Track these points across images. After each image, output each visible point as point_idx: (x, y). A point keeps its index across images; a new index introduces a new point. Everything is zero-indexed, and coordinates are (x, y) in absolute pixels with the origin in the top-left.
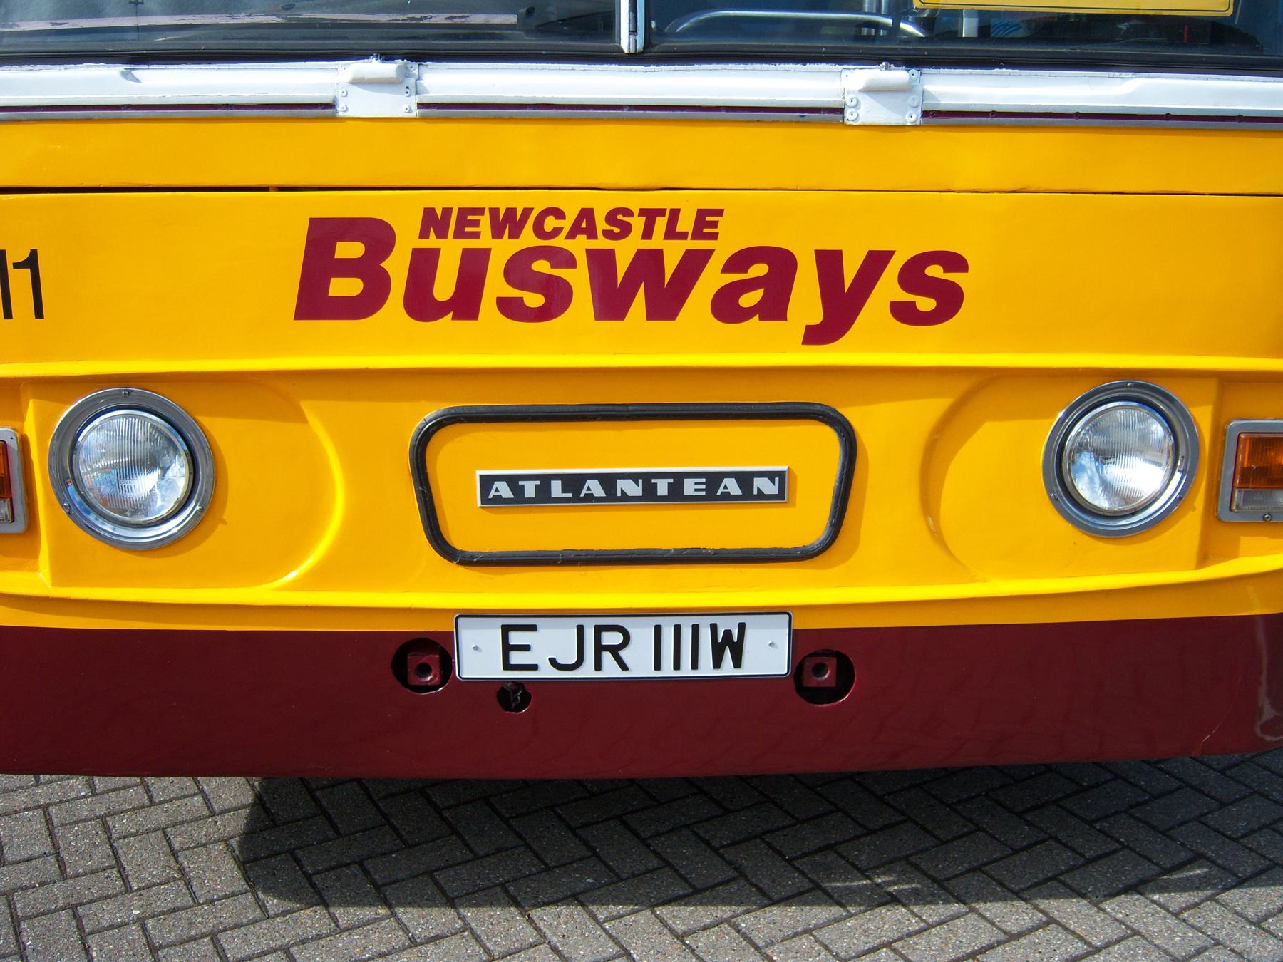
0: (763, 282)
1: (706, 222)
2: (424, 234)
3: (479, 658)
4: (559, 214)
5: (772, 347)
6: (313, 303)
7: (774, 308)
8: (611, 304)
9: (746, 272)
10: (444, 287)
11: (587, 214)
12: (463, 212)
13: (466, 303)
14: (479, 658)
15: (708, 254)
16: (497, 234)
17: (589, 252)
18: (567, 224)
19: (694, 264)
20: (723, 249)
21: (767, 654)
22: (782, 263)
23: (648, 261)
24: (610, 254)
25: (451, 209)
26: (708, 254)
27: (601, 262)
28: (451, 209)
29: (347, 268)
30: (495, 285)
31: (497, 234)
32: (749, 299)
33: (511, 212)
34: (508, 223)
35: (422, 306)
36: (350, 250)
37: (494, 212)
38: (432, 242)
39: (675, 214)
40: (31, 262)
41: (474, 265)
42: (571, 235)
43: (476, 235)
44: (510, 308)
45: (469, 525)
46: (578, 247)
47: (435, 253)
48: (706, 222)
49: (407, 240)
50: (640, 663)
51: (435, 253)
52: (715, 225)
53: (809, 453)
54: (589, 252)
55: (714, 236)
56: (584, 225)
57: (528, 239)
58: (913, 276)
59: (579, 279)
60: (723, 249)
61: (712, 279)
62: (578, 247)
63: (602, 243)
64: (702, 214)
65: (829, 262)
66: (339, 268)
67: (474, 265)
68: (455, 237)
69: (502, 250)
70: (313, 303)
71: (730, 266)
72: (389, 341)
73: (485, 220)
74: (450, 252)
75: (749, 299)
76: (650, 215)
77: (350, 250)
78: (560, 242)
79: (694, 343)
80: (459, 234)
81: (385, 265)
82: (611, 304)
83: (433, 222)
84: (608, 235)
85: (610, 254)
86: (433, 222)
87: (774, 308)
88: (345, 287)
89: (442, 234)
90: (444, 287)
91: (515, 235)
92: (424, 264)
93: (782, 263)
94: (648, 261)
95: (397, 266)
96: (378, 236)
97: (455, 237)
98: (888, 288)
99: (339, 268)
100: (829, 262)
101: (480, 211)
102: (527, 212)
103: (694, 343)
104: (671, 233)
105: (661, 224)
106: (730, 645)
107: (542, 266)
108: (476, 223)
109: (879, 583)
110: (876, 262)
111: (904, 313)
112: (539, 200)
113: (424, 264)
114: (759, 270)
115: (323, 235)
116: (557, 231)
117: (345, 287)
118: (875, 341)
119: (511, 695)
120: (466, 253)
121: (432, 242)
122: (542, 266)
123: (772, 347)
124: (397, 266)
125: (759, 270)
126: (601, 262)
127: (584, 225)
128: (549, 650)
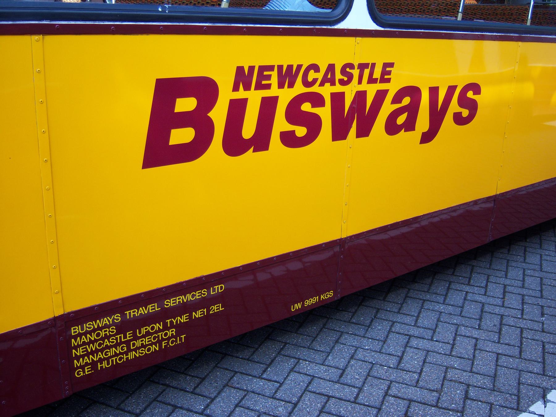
2: (236, 88)
4: (316, 68)
9: (400, 102)
11: (331, 68)
12: (262, 69)
13: (261, 142)
15: (385, 92)
16: (281, 85)
17: (332, 94)
18: (320, 76)
24: (342, 94)
25: (254, 67)
26: (385, 92)
28: (254, 67)
29: (184, 120)
30: (281, 124)
31: (281, 85)
32: (401, 120)
33: (290, 67)
35: (235, 145)
36: (186, 104)
37: (280, 67)
38: (241, 94)
39: (374, 65)
42: (322, 84)
43: (268, 87)
44: (289, 140)
46: (326, 91)
47: (245, 101)
51: (245, 101)
52: (389, 73)
54: (332, 94)
55: (388, 81)
56: (329, 76)
57: (299, 89)
59: (325, 113)
60: (393, 88)
62: (326, 91)
63: (338, 88)
64: (386, 65)
68: (256, 89)
70: (158, 153)
71: (394, 101)
73: (274, 74)
75: (401, 120)
76: (362, 67)
77: (186, 104)
78: (315, 89)
80: (259, 86)
81: (209, 115)
83: (242, 78)
84: (342, 82)
85: (342, 94)
86: (242, 78)
88: (182, 136)
89: (247, 88)
91: (291, 85)
95: (219, 115)
96: (205, 90)
97: (256, 89)
98: (454, 107)
101: (271, 68)
102: (299, 67)
104: (371, 80)
105: (367, 72)
107: (306, 107)
108: (269, 77)
114: (406, 101)
116: (315, 81)
117: (182, 136)
120: (265, 101)
121: (241, 94)
122: (306, 107)
124: (219, 115)
125: (406, 101)
127: (329, 76)
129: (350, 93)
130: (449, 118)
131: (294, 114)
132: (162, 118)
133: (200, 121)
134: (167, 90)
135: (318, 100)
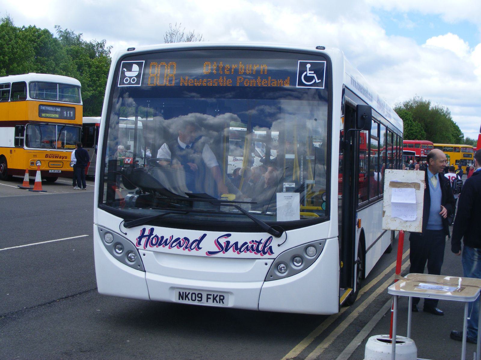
0: (60, 157)
1: (59, 155)
3: (50, 172)
5: (61, 159)
6: (46, 157)
7: (61, 158)
8: (56, 158)
13: (51, 157)
14: (50, 172)
19: (58, 156)
20: (59, 156)
21: (60, 172)
22: (61, 156)
30: (52, 157)
35: (49, 157)
45: (50, 166)
48: (59, 155)
53: (61, 164)
58: (65, 157)
60: (59, 156)
61: (59, 157)
65: (63, 157)
66: (47, 156)
70: (46, 157)
72: (48, 159)
74: (50, 156)
79: (58, 159)
82: (56, 158)
87: (61, 158)
92: (49, 156)
93: (61, 156)
94: (57, 156)
96: (48, 155)
99: (47, 156)
100: (63, 157)
103: (58, 159)
106: (59, 171)
109: (63, 169)
110: (64, 157)
111: (65, 158)
113: (49, 156)
115: (46, 155)
118: (64, 159)
123: (61, 159)
128: (53, 171)
129: (56, 156)
130: (64, 158)
132: (46, 156)
133: (48, 156)
134: (46, 155)
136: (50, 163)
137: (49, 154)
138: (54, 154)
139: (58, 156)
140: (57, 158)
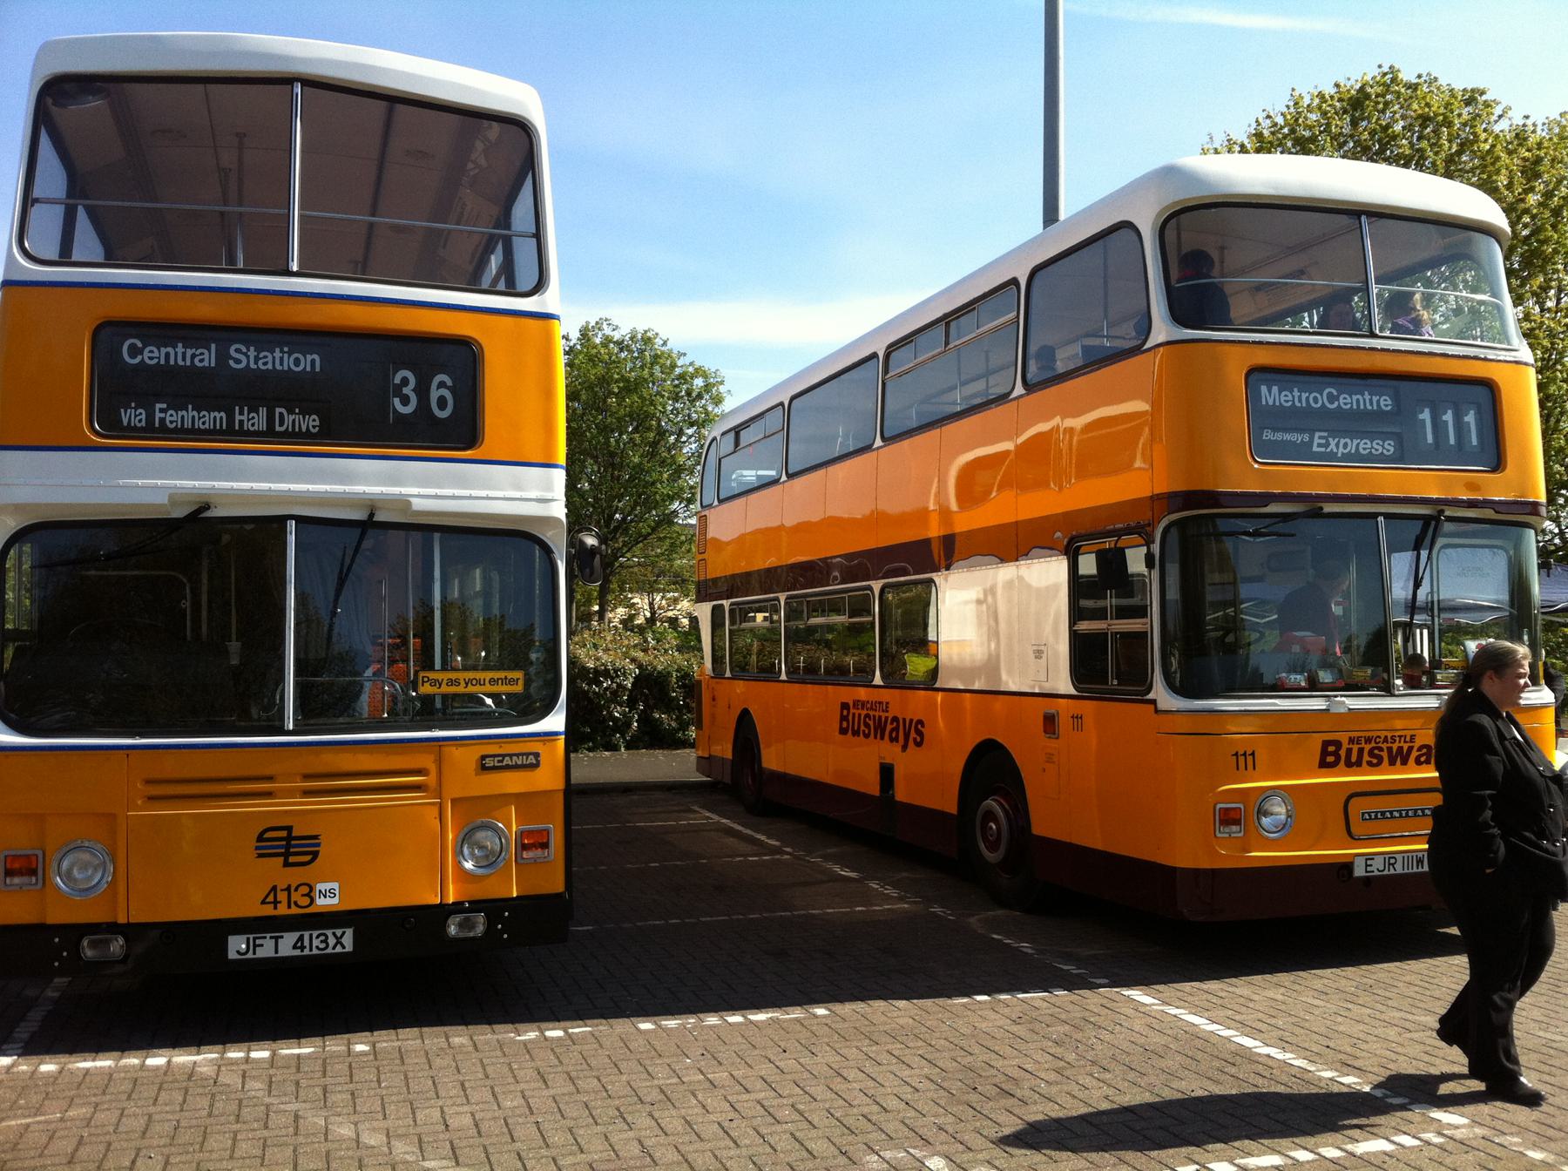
6: (1323, 764)
10: (1354, 759)
13: (1359, 763)
14: (1359, 871)
19: (1410, 749)
23: (1401, 748)
27: (1390, 749)
29: (1331, 754)
30: (1366, 758)
34: (1368, 740)
35: (1349, 764)
36: (1331, 749)
40: (1253, 754)
41: (1361, 751)
44: (1370, 764)
46: (1384, 746)
48: (1413, 737)
49: (1345, 746)
50: (1399, 870)
59: (1385, 754)
61: (1415, 754)
62: (1384, 746)
67: (1361, 751)
69: (1367, 747)
74: (1355, 748)
77: (1331, 749)
82: (1392, 763)
83: (1351, 741)
86: (1351, 741)
88: (1330, 759)
90: (1354, 759)
92: (1349, 751)
94: (1401, 748)
95: (1343, 753)
96: (1338, 744)
112: (1375, 734)
113: (1349, 751)
115: (1326, 744)
117: (1330, 759)
119: (1367, 881)
124: (1343, 753)
126: (1390, 749)
128: (1377, 865)
129: (1395, 747)
131: (1371, 753)
132: (1324, 753)
133: (1336, 754)
135: (1381, 749)
136: (1357, 807)
137: (1343, 738)
138: (1383, 734)
139: (1410, 749)
140: (1404, 762)
